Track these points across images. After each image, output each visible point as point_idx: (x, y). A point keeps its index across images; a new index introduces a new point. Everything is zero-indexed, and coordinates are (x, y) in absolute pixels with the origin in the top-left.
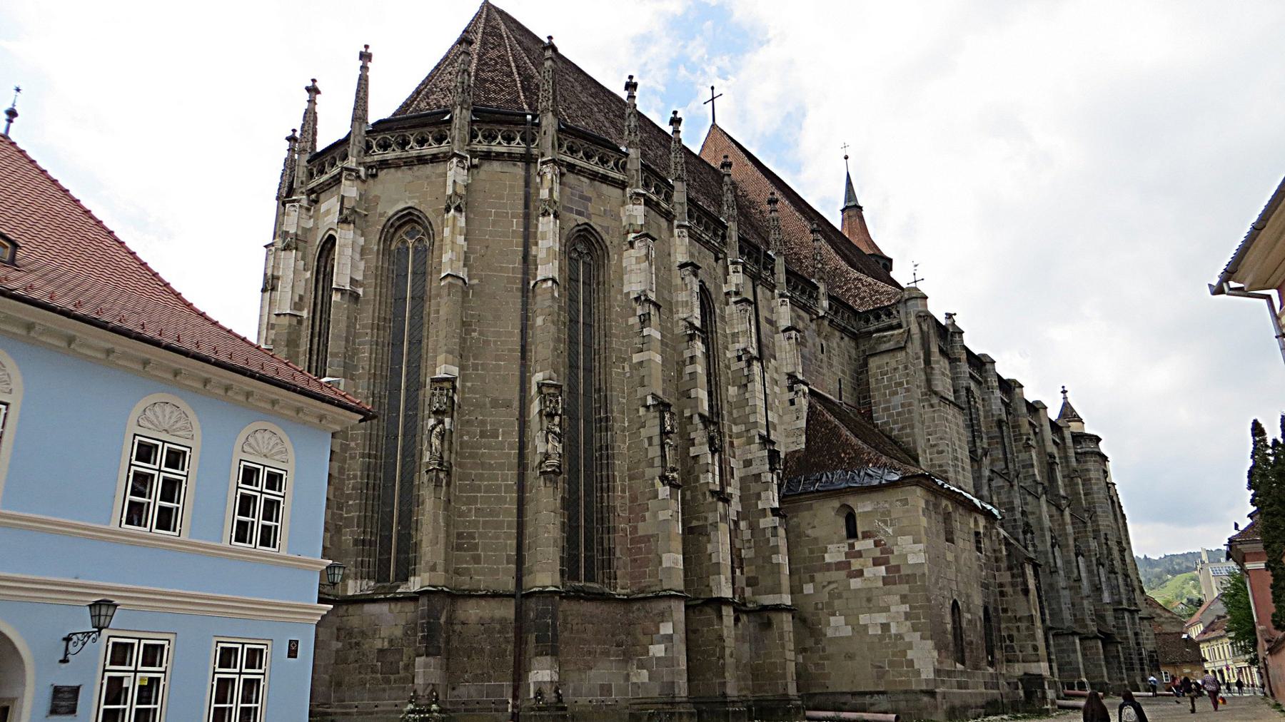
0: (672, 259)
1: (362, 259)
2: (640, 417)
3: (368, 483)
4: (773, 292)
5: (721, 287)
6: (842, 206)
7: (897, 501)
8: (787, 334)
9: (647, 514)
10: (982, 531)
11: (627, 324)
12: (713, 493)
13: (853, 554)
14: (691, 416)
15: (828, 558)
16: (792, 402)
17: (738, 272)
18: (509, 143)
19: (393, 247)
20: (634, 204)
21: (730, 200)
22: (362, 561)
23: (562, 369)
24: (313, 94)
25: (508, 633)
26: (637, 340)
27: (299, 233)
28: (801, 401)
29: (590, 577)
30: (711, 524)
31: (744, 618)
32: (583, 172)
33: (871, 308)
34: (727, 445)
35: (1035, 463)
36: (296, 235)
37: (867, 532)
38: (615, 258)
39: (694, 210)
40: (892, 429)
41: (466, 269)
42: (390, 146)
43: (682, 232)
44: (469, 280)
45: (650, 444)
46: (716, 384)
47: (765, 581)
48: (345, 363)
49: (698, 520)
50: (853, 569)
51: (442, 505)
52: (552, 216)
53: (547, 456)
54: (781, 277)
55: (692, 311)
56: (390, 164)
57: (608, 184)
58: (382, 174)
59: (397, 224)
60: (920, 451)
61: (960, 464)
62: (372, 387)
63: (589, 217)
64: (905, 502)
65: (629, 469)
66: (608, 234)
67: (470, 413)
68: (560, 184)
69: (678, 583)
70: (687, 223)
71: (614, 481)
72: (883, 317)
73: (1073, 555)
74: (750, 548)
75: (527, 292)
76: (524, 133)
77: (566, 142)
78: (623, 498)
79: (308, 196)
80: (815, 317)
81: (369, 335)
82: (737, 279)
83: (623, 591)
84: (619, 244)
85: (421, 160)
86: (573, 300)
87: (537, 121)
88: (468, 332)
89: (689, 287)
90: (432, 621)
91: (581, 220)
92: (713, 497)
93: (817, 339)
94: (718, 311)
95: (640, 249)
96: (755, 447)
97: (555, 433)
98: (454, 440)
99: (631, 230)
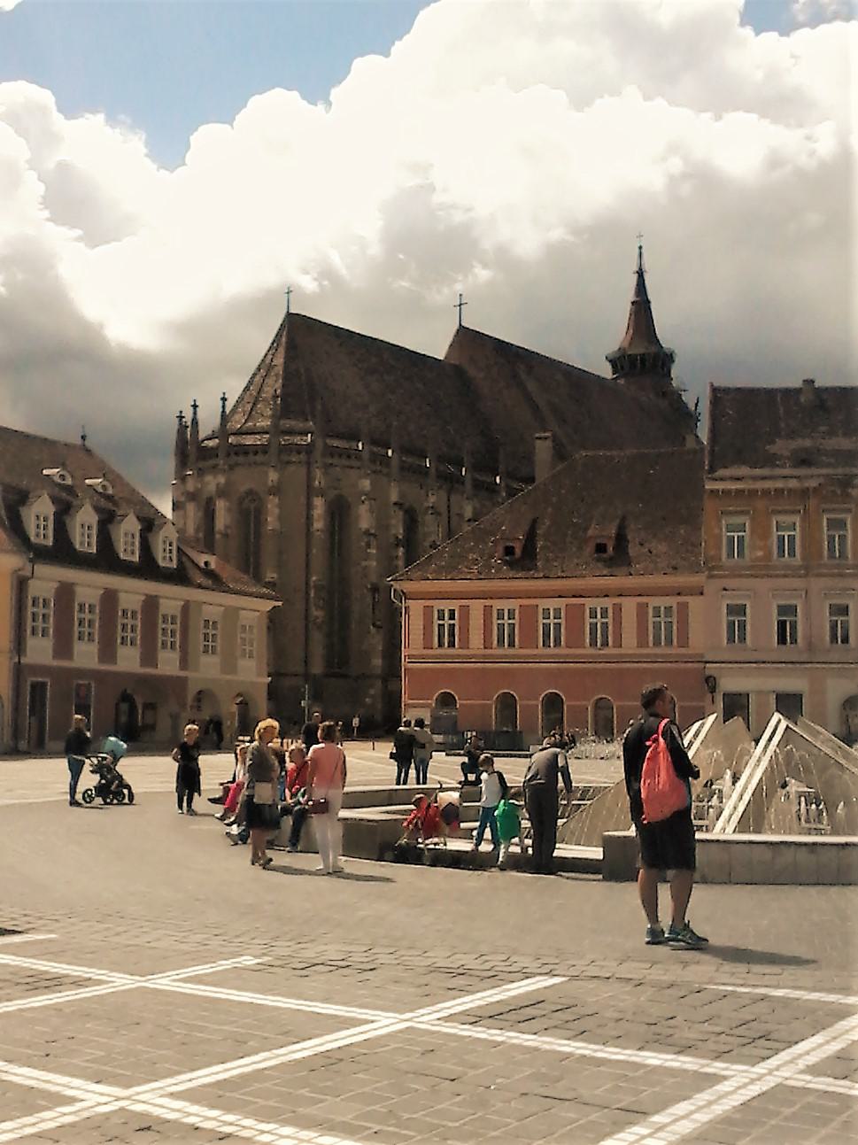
53: (317, 617)
69: (379, 671)
75: (309, 534)
91: (336, 492)
94: (420, 519)
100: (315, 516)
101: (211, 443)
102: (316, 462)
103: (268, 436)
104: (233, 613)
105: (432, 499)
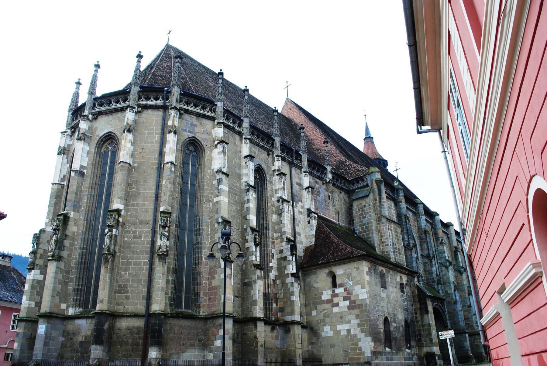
0: (241, 154)
1: (87, 156)
2: (215, 228)
3: (81, 262)
4: (301, 170)
5: (270, 168)
6: (364, 138)
7: (354, 268)
9: (216, 276)
10: (405, 282)
11: (212, 184)
13: (335, 295)
14: (247, 228)
15: (324, 298)
16: (309, 222)
17: (279, 160)
18: (157, 101)
19: (102, 151)
20: (218, 127)
21: (276, 127)
22: (76, 298)
23: (176, 206)
24: (78, 85)
25: (141, 334)
26: (216, 191)
27: (66, 146)
28: (313, 221)
29: (187, 306)
30: (253, 281)
32: (192, 113)
33: (355, 178)
34: (270, 243)
35: (446, 251)
36: (64, 147)
37: (341, 284)
38: (207, 153)
39: (255, 131)
40: (363, 235)
41: (132, 159)
43: (247, 141)
44: (133, 164)
46: (266, 213)
47: (288, 310)
48: (74, 204)
49: (248, 278)
50: (334, 302)
51: (108, 271)
52: (173, 133)
53: (160, 247)
54: (305, 163)
56: (103, 113)
57: (206, 119)
59: (104, 140)
60: (376, 245)
61: (397, 251)
62: (87, 216)
64: (358, 268)
66: (205, 142)
67: (129, 226)
68: (179, 118)
70: (249, 137)
71: (201, 259)
72: (361, 182)
73: (467, 294)
75: (160, 168)
76: (163, 96)
77: (184, 99)
78: (206, 268)
79: (71, 129)
80: (325, 182)
81: (88, 191)
82: (278, 164)
83: (204, 314)
84: (210, 146)
85: (116, 110)
86: (184, 173)
87: (169, 90)
88: (131, 189)
89: (248, 167)
90: (99, 327)
91: (191, 135)
92: (254, 267)
93: (326, 193)
94: (268, 179)
95: (220, 148)
96: (284, 244)
97: (165, 235)
98: (119, 239)
99: (216, 140)
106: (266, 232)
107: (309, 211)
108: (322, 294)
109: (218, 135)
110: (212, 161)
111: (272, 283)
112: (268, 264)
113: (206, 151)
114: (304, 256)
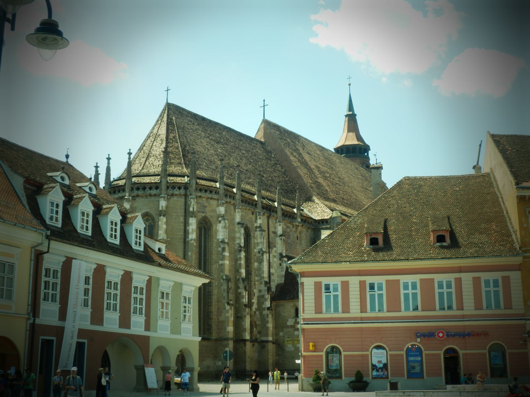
2: (221, 282)
4: (276, 220)
5: (254, 225)
8: (280, 238)
9: (222, 314)
12: (245, 305)
14: (239, 279)
16: (280, 265)
17: (261, 219)
18: (179, 190)
26: (221, 256)
31: (256, 344)
33: (320, 219)
34: (253, 285)
38: (214, 226)
42: (140, 189)
45: (224, 292)
46: (250, 263)
55: (241, 241)
58: (137, 199)
63: (206, 213)
65: (217, 299)
69: (231, 335)
71: (212, 303)
74: (259, 321)
75: (185, 242)
85: (150, 195)
91: (203, 215)
94: (252, 235)
96: (263, 286)
100: (190, 231)
101: (122, 183)
102: (191, 194)
103: (159, 177)
104: (178, 286)
105: (259, 221)
106: (250, 277)
107: (281, 254)
108: (287, 321)
109: (221, 213)
110: (218, 233)
111: (253, 314)
112: (251, 301)
113: (213, 225)
114: (276, 291)
